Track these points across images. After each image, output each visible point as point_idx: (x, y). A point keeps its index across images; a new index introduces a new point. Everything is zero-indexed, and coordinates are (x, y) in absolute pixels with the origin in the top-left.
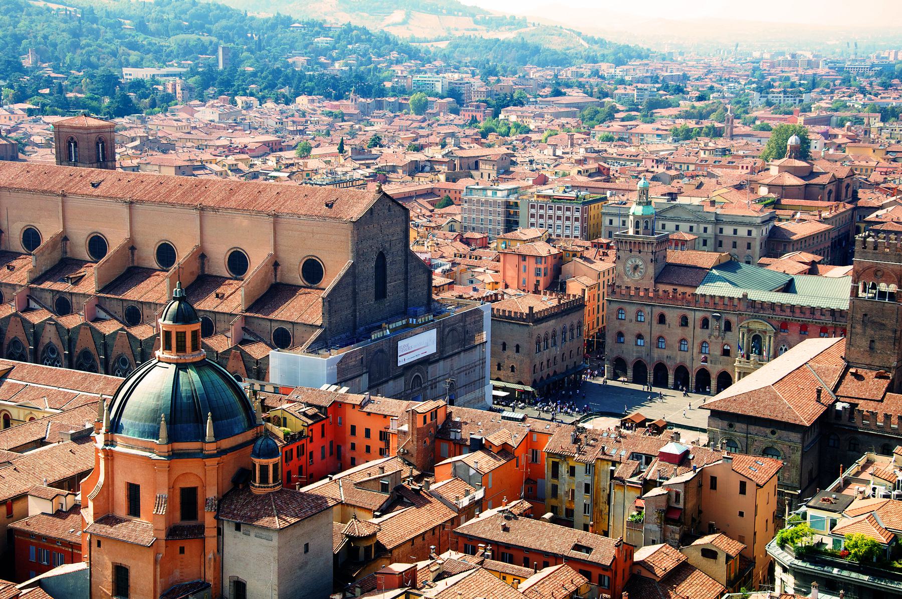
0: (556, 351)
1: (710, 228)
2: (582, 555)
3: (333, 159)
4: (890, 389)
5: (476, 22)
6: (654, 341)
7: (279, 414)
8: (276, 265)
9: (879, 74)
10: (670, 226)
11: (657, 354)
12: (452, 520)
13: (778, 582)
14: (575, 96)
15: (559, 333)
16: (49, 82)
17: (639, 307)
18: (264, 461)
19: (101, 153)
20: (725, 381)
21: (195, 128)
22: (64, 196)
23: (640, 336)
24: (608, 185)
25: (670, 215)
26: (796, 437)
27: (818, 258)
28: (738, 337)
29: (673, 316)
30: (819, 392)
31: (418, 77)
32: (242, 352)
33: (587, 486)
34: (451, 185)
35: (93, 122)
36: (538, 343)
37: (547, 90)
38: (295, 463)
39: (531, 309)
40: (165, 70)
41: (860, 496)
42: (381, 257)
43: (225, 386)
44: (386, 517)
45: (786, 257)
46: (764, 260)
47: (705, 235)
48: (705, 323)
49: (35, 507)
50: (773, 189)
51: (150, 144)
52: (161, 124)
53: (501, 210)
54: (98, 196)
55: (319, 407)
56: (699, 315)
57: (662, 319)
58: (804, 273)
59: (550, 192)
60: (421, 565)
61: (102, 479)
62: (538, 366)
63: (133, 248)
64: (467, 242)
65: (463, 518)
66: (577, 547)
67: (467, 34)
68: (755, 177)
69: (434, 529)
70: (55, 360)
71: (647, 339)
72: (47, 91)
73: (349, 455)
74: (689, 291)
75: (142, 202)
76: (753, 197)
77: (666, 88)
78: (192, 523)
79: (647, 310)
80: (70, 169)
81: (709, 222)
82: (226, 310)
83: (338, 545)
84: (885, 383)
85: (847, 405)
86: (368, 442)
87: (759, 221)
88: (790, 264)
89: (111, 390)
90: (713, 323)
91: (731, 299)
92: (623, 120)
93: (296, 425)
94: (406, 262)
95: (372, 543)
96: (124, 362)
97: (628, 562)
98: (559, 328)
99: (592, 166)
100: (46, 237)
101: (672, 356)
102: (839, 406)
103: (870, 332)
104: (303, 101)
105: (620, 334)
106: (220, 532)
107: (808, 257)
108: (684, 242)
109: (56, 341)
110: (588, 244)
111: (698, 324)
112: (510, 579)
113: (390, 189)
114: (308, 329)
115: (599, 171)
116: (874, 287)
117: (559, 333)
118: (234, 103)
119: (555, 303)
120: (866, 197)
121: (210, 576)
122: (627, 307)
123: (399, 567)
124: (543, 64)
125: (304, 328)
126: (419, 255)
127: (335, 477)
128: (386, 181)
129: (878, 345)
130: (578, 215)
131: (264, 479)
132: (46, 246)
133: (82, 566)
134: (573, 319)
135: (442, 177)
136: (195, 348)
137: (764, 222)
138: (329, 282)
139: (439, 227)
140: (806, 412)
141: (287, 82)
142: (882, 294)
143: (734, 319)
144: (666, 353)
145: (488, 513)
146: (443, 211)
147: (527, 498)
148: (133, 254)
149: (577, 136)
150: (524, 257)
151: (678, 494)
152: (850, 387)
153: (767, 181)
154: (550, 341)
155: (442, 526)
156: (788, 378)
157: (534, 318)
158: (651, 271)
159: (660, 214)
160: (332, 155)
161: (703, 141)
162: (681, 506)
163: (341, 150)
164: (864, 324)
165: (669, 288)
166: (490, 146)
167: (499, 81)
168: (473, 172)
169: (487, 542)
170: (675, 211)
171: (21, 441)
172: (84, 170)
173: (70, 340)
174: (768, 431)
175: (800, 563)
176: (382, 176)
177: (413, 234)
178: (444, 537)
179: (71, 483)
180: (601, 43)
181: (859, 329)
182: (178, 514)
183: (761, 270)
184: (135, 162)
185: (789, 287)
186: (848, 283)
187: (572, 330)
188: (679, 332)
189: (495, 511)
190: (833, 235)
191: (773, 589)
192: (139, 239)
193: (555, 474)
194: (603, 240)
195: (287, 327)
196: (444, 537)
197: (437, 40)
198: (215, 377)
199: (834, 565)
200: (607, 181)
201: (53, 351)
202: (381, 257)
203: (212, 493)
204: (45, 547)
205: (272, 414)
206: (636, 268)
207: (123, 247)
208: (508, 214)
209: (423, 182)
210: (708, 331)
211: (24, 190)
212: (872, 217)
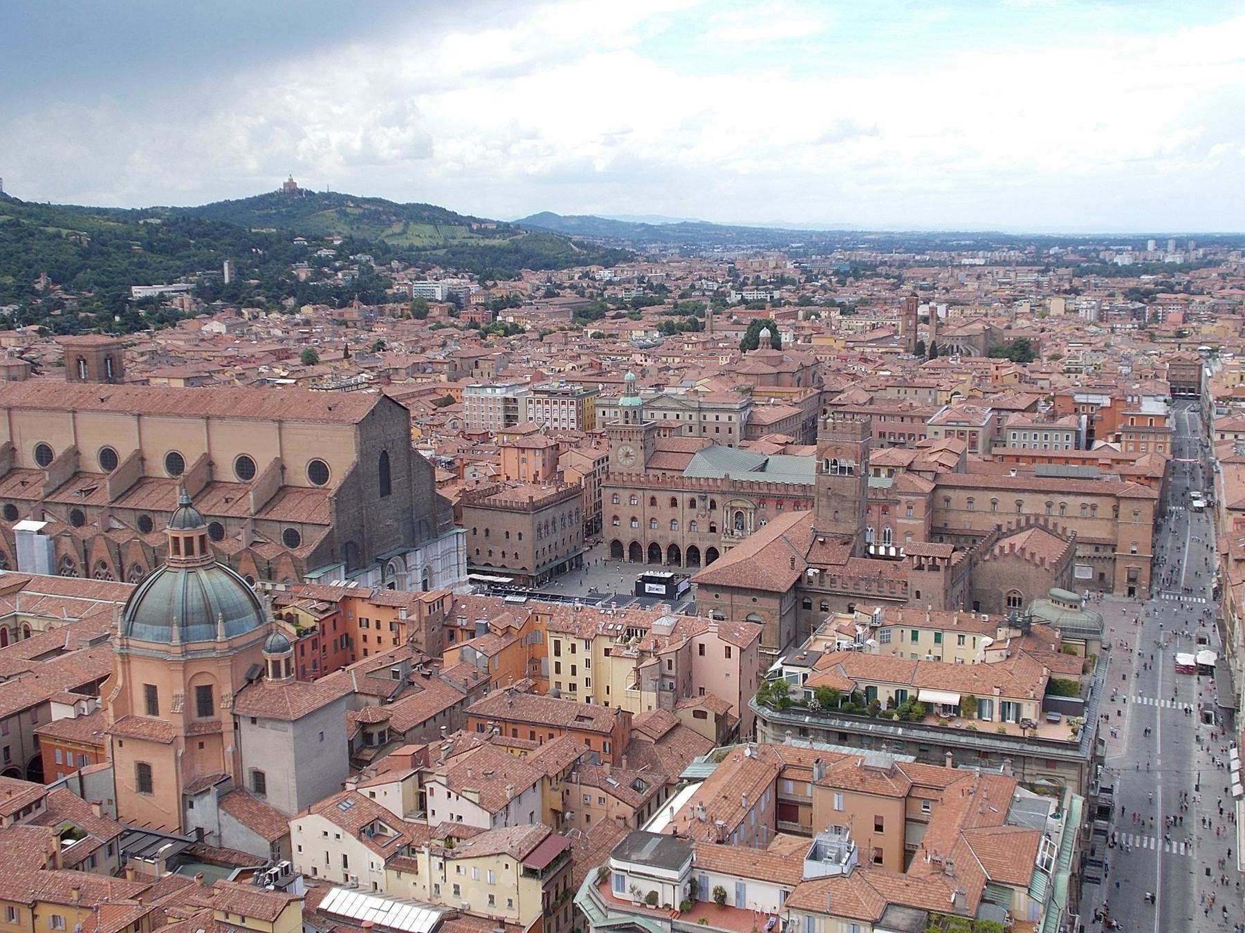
0: (557, 537)
1: (694, 415)
2: (587, 724)
3: (338, 364)
4: (852, 554)
5: (472, 231)
6: (648, 522)
7: (290, 610)
8: (283, 468)
9: (836, 273)
10: (659, 415)
11: (653, 535)
12: (462, 701)
13: (759, 733)
14: (569, 296)
15: (558, 519)
16: (60, 304)
17: (632, 492)
18: (276, 656)
19: (111, 370)
20: (713, 554)
21: (202, 340)
22: (74, 412)
23: (634, 519)
24: (600, 379)
25: (657, 404)
26: (774, 604)
27: (790, 439)
28: (721, 517)
29: (663, 498)
30: (793, 560)
31: (418, 285)
32: (253, 554)
33: (588, 661)
34: (453, 385)
35: (102, 339)
36: (539, 530)
37: (541, 293)
38: (308, 659)
39: (531, 498)
40: (171, 288)
41: (827, 651)
42: (385, 455)
43: (235, 587)
44: (396, 704)
45: (762, 440)
46: (745, 443)
47: (690, 422)
48: (693, 504)
49: (59, 712)
50: (750, 377)
51: (158, 357)
52: (165, 339)
53: (501, 405)
54: (107, 411)
55: (331, 603)
56: (687, 496)
57: (653, 501)
58: (779, 453)
59: (546, 388)
60: (432, 746)
61: (120, 682)
62: (540, 553)
63: (143, 459)
64: (469, 437)
65: (472, 699)
66: (580, 718)
67: (465, 241)
68: (734, 367)
69: (444, 711)
70: (72, 570)
71: (641, 520)
72: (58, 312)
73: (361, 646)
74: (676, 474)
75: (149, 414)
76: (732, 385)
77: (651, 287)
78: (210, 718)
79: (640, 493)
80: (77, 386)
81: (693, 409)
82: (235, 514)
83: (354, 732)
84: (848, 549)
85: (817, 571)
86: (379, 633)
87: (738, 407)
88: (766, 445)
89: (127, 598)
90: (699, 503)
91: (715, 480)
92: (613, 318)
93: (308, 620)
94: (409, 460)
95: (385, 727)
96: (139, 569)
97: (627, 729)
98: (558, 515)
99: (584, 360)
100: (58, 452)
101: (664, 535)
102: (810, 572)
103: (833, 503)
104: (307, 310)
105: (616, 518)
106: (236, 726)
107: (782, 438)
108: (671, 429)
109: (72, 553)
110: (583, 434)
111: (687, 504)
112: (517, 752)
113: (391, 392)
114: (317, 528)
115: (591, 366)
116: (835, 463)
117: (558, 519)
118: (241, 315)
119: (553, 491)
120: (831, 382)
121: (230, 770)
122: (621, 492)
123: (411, 749)
124: (535, 268)
125: (312, 528)
126: (421, 452)
127: (348, 668)
128: (389, 381)
129: (840, 515)
130: (573, 407)
131: (277, 674)
132: (59, 460)
133: (107, 765)
134: (572, 506)
135: (444, 378)
136: (203, 551)
137: (743, 409)
138: (334, 482)
139: (442, 425)
140: (784, 580)
141: (292, 293)
142: (842, 469)
143: (718, 498)
144: (659, 533)
145: (494, 693)
146: (444, 409)
147: (531, 676)
148: (143, 465)
149: (570, 333)
150: (523, 449)
151: (670, 662)
152: (820, 555)
153: (743, 371)
154: (550, 528)
155: (453, 707)
156: (763, 550)
157: (535, 507)
158: (641, 457)
159: (647, 405)
160: (338, 360)
161: (686, 335)
162: (673, 672)
163: (347, 356)
164: (829, 497)
165: (659, 473)
166: (486, 346)
167: (495, 285)
168: (475, 371)
169: (495, 719)
170: (663, 400)
171: (42, 649)
172: (93, 386)
173: (85, 551)
174: (749, 599)
175: (777, 715)
176: (386, 377)
177: (416, 432)
178: (453, 718)
179: (90, 689)
180: (591, 247)
181: (824, 502)
182: (195, 712)
183: (741, 452)
184: (145, 376)
185: (763, 468)
186: (813, 461)
187: (570, 516)
188: (670, 513)
189: (501, 691)
190: (804, 418)
191: (755, 740)
192: (148, 451)
193: (557, 653)
194: (598, 429)
195: (296, 528)
196: (453, 718)
197: (435, 248)
198: (225, 579)
199: (807, 713)
200: (599, 375)
201: (70, 562)
202: (385, 455)
203: (228, 690)
204: (69, 750)
205: (284, 612)
206: (627, 455)
207: (132, 458)
208: (506, 409)
209: (425, 382)
210: (695, 511)
211: (35, 408)
212: (835, 400)
